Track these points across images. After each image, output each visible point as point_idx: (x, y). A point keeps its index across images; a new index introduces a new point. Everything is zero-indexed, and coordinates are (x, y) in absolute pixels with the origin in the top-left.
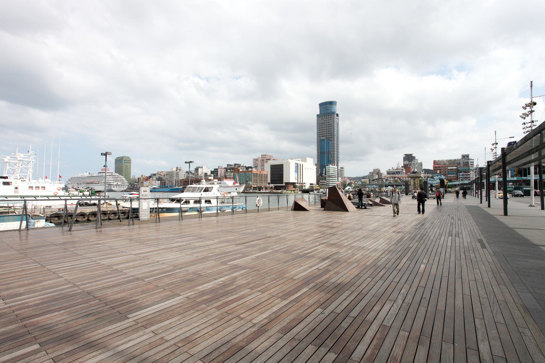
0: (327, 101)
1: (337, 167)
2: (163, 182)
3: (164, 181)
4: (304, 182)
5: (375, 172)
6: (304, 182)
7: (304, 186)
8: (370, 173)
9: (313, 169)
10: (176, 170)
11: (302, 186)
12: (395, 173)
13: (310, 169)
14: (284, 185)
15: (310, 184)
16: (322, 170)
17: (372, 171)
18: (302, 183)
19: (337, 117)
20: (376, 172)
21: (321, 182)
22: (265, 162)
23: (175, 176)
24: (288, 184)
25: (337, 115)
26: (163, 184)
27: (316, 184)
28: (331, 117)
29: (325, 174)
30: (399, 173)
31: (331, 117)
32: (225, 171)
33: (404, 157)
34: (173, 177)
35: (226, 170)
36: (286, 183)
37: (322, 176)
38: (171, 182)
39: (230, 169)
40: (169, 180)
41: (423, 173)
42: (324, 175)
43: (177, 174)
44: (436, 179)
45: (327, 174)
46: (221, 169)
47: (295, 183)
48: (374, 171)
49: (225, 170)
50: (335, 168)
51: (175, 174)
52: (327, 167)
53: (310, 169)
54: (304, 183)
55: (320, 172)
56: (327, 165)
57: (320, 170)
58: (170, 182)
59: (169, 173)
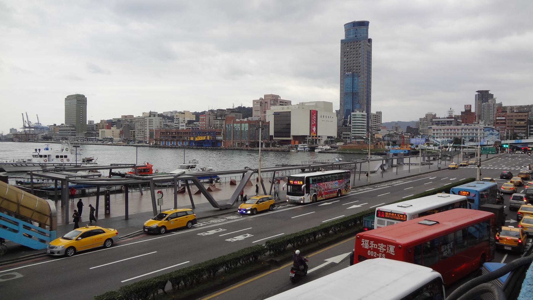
0: (356, 21)
1: (366, 114)
2: (131, 132)
3: (134, 130)
4: (318, 135)
5: (428, 117)
6: (318, 135)
7: (319, 140)
8: (421, 119)
9: (333, 117)
10: (150, 116)
11: (316, 140)
12: (445, 123)
13: (327, 117)
14: (291, 138)
15: (328, 137)
16: (346, 117)
17: (423, 116)
18: (316, 137)
19: (369, 44)
20: (429, 118)
21: (344, 134)
22: (269, 104)
23: (148, 123)
24: (295, 137)
25: (370, 41)
26: (132, 134)
27: (336, 137)
28: (360, 43)
29: (350, 123)
30: (451, 124)
31: (360, 43)
32: (215, 118)
33: (476, 95)
34: (146, 126)
35: (216, 118)
36: (294, 136)
37: (346, 126)
38: (143, 131)
39: (221, 116)
40: (140, 129)
41: (482, 123)
42: (348, 124)
43: (151, 121)
44: (487, 134)
45: (353, 123)
46: (209, 116)
47: (306, 136)
48: (426, 116)
49: (215, 116)
50: (364, 115)
51: (148, 121)
52: (352, 113)
53: (327, 117)
54: (319, 136)
55: (343, 120)
56: (353, 111)
57: (343, 117)
58: (141, 132)
59: (139, 120)
